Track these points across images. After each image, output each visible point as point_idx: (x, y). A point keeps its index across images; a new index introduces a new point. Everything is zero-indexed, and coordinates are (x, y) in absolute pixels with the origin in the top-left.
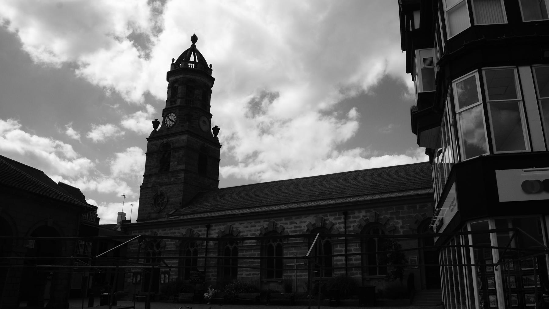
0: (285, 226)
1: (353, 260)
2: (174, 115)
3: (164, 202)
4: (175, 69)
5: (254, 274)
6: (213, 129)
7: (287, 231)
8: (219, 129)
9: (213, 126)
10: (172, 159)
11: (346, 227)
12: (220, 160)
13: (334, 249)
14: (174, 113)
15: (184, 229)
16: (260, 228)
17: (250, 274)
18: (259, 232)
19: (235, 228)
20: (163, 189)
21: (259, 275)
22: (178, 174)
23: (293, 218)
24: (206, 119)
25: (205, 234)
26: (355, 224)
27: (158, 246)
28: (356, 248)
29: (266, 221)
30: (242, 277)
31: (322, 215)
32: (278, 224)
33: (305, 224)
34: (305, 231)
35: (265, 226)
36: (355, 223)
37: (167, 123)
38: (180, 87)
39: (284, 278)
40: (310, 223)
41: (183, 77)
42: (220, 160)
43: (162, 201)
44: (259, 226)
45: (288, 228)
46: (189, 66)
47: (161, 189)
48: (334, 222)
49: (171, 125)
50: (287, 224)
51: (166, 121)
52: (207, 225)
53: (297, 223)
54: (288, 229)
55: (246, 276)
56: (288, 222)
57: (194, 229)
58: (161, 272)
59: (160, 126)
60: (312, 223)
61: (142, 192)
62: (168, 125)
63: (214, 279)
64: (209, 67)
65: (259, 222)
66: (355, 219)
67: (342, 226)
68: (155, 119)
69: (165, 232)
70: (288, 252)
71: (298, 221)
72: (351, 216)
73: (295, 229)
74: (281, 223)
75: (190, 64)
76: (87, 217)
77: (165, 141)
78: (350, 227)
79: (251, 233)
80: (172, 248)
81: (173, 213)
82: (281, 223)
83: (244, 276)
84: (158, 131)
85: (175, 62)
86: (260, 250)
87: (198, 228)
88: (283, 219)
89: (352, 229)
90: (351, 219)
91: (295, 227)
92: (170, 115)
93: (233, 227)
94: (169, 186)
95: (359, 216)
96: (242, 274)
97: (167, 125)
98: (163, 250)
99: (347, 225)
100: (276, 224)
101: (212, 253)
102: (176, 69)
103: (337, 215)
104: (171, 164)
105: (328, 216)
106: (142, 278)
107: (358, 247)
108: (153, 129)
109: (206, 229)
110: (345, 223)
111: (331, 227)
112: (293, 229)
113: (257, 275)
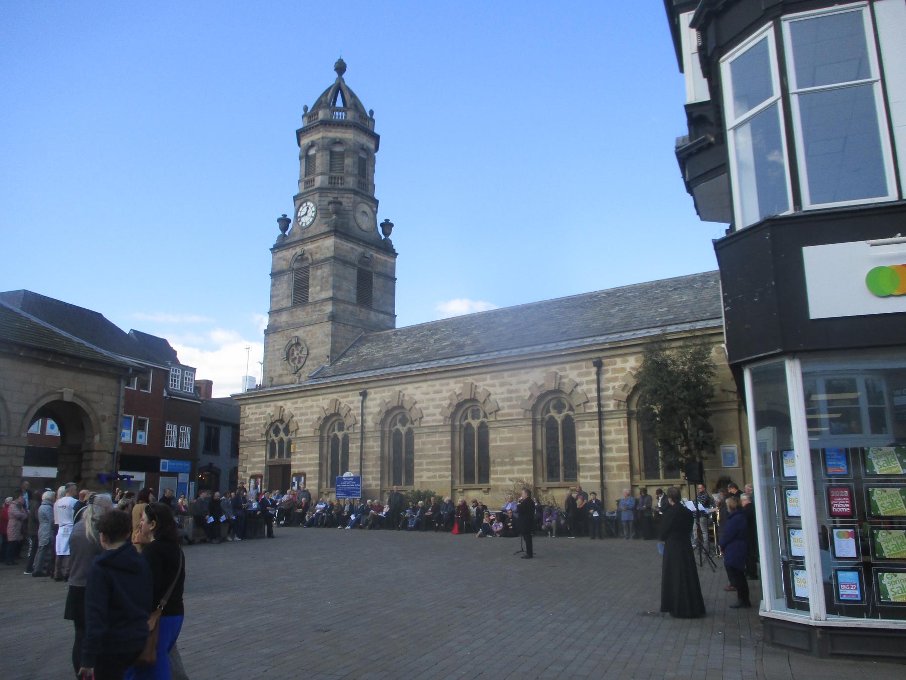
0: (491, 390)
1: (614, 450)
3: (303, 356)
4: (309, 124)
5: (440, 477)
6: (382, 225)
7: (496, 399)
8: (392, 225)
9: (380, 220)
10: (311, 281)
11: (599, 390)
12: (396, 279)
13: (579, 430)
15: (326, 400)
16: (450, 393)
17: (434, 477)
18: (448, 402)
19: (408, 395)
20: (300, 333)
21: (450, 477)
22: (323, 307)
23: (506, 374)
24: (366, 208)
25: (359, 407)
26: (617, 384)
27: (287, 431)
28: (618, 427)
29: (459, 382)
30: (422, 482)
31: (558, 369)
32: (480, 386)
33: (527, 386)
34: (527, 398)
35: (458, 392)
36: (617, 381)
38: (319, 155)
39: (492, 483)
40: (536, 384)
41: (323, 138)
42: (396, 279)
43: (300, 355)
44: (447, 391)
45: (496, 394)
46: (335, 116)
47: (297, 334)
48: (578, 380)
49: (308, 224)
50: (493, 386)
52: (361, 391)
53: (511, 385)
54: (496, 396)
55: (428, 480)
56: (497, 382)
57: (341, 400)
58: (292, 474)
59: (291, 225)
60: (539, 384)
61: (266, 341)
62: (302, 223)
63: (376, 485)
64: (368, 115)
65: (448, 384)
66: (617, 375)
67: (595, 386)
68: (282, 215)
69: (296, 406)
70: (498, 436)
71: (513, 380)
72: (610, 368)
73: (509, 395)
74: (483, 386)
75: (337, 113)
76: (179, 386)
77: (298, 250)
78: (607, 389)
79: (434, 403)
80: (307, 432)
81: (315, 374)
82: (483, 386)
83: (424, 479)
84: (287, 235)
85: (309, 111)
86: (450, 434)
87: (347, 397)
88: (488, 376)
89: (610, 392)
90: (609, 375)
91: (510, 392)
92: (305, 205)
93: (404, 395)
94: (308, 328)
95: (624, 368)
96: (421, 477)
98: (294, 436)
99: (603, 385)
100: (476, 386)
101: (371, 440)
102: (311, 123)
103: (584, 367)
104: (310, 290)
105: (566, 370)
106: (263, 484)
107: (622, 427)
108: (280, 232)
109: (361, 398)
110: (598, 382)
111: (572, 391)
112: (506, 395)
113: (447, 477)
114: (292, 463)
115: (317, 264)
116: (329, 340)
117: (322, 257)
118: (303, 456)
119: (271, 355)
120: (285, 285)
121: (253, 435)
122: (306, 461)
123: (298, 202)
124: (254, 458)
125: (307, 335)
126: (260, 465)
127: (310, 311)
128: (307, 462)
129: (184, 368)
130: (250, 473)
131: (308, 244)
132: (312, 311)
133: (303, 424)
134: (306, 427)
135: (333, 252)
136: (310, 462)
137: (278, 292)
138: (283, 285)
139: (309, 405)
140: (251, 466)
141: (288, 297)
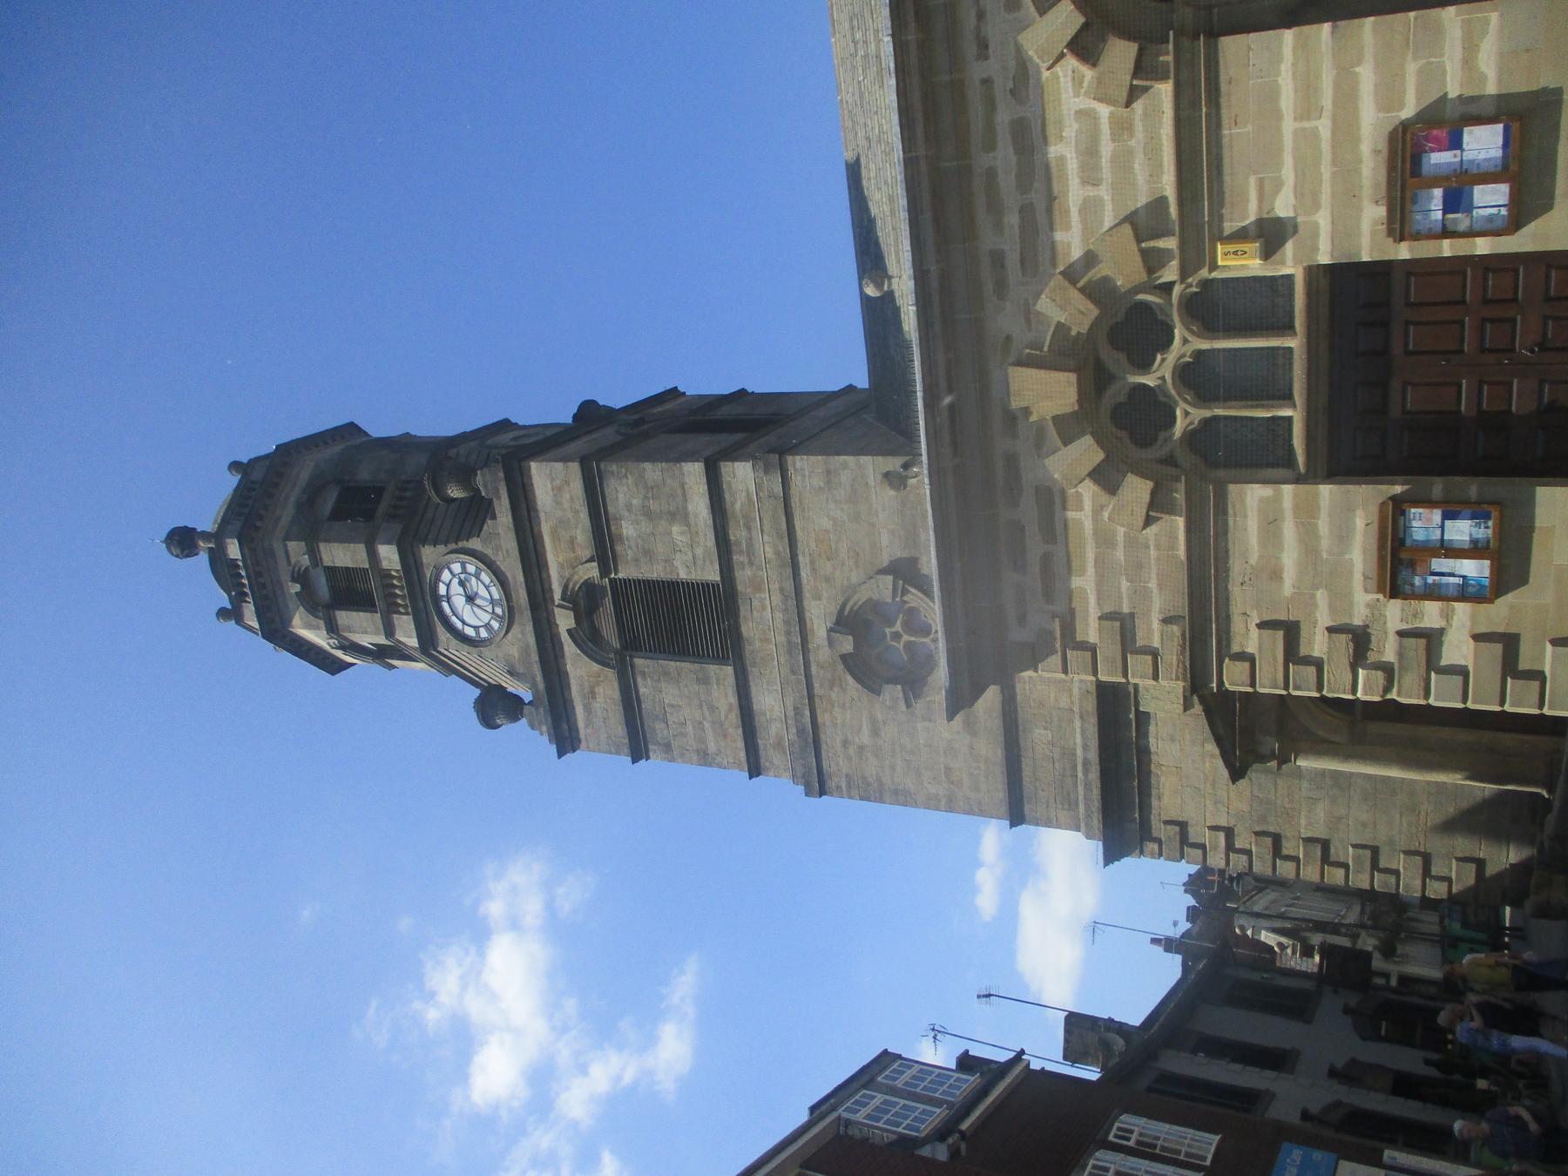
2: (446, 576)
10: (655, 572)
14: (437, 579)
20: (820, 617)
22: (738, 506)
37: (487, 626)
51: (476, 628)
69: (1012, 260)
77: (564, 621)
80: (1153, 153)
97: (495, 625)
104: (683, 575)
114: (1324, 259)
115: (604, 546)
116: (845, 466)
117: (584, 516)
118: (1288, 173)
119: (893, 768)
120: (670, 694)
121: (1153, 585)
122: (1314, 134)
123: (442, 634)
124: (1276, 575)
125: (827, 580)
126: (1323, 526)
127: (749, 572)
128: (1324, 127)
129: (866, 1078)
130: (1362, 602)
131: (546, 586)
132: (751, 563)
133: (1104, 192)
134: (1122, 163)
135: (570, 464)
136: (1327, 101)
137: (690, 729)
138: (667, 701)
139: (1013, 159)
140: (1321, 596)
141: (704, 681)
